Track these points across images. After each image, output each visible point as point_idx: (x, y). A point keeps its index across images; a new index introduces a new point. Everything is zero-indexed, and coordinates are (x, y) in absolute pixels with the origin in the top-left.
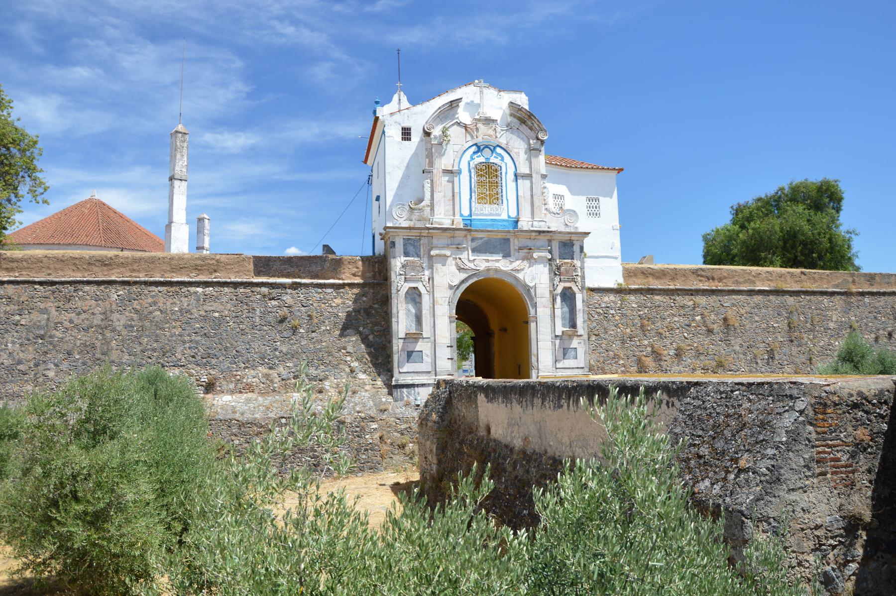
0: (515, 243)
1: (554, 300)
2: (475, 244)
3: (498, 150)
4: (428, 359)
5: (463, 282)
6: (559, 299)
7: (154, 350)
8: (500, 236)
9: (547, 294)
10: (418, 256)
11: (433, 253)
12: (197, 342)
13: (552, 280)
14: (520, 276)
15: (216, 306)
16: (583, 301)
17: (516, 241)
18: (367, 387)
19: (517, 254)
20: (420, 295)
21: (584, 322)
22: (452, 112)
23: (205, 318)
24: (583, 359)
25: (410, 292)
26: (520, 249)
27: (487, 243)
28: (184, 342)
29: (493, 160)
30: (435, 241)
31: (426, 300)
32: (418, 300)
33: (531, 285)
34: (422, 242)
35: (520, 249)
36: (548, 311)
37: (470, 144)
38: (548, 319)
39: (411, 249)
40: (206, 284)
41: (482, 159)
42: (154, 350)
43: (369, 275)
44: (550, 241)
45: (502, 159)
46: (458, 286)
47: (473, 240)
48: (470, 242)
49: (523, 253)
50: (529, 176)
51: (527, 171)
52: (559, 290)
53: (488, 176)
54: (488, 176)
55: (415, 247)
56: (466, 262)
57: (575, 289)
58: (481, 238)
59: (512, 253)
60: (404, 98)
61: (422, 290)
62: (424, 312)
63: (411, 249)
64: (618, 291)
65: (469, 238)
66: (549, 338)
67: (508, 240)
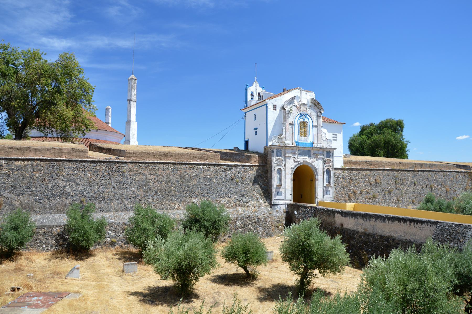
0: (312, 152)
1: (324, 173)
2: (299, 152)
3: (307, 116)
4: (283, 195)
6: (325, 173)
7: (187, 191)
9: (322, 171)
10: (281, 156)
12: (203, 188)
13: (323, 166)
14: (313, 164)
15: (208, 173)
18: (263, 205)
20: (281, 171)
23: (205, 178)
26: (314, 154)
27: (303, 151)
28: (198, 188)
29: (306, 120)
30: (287, 151)
31: (283, 172)
33: (317, 167)
35: (314, 154)
36: (322, 177)
37: (298, 113)
38: (322, 180)
39: (279, 153)
40: (204, 165)
41: (302, 120)
42: (187, 191)
43: (260, 162)
47: (299, 150)
49: (315, 155)
50: (317, 126)
51: (316, 125)
52: (325, 170)
53: (304, 125)
54: (304, 125)
57: (330, 169)
60: (258, 84)
61: (282, 169)
63: (279, 153)
64: (342, 169)
67: (310, 151)
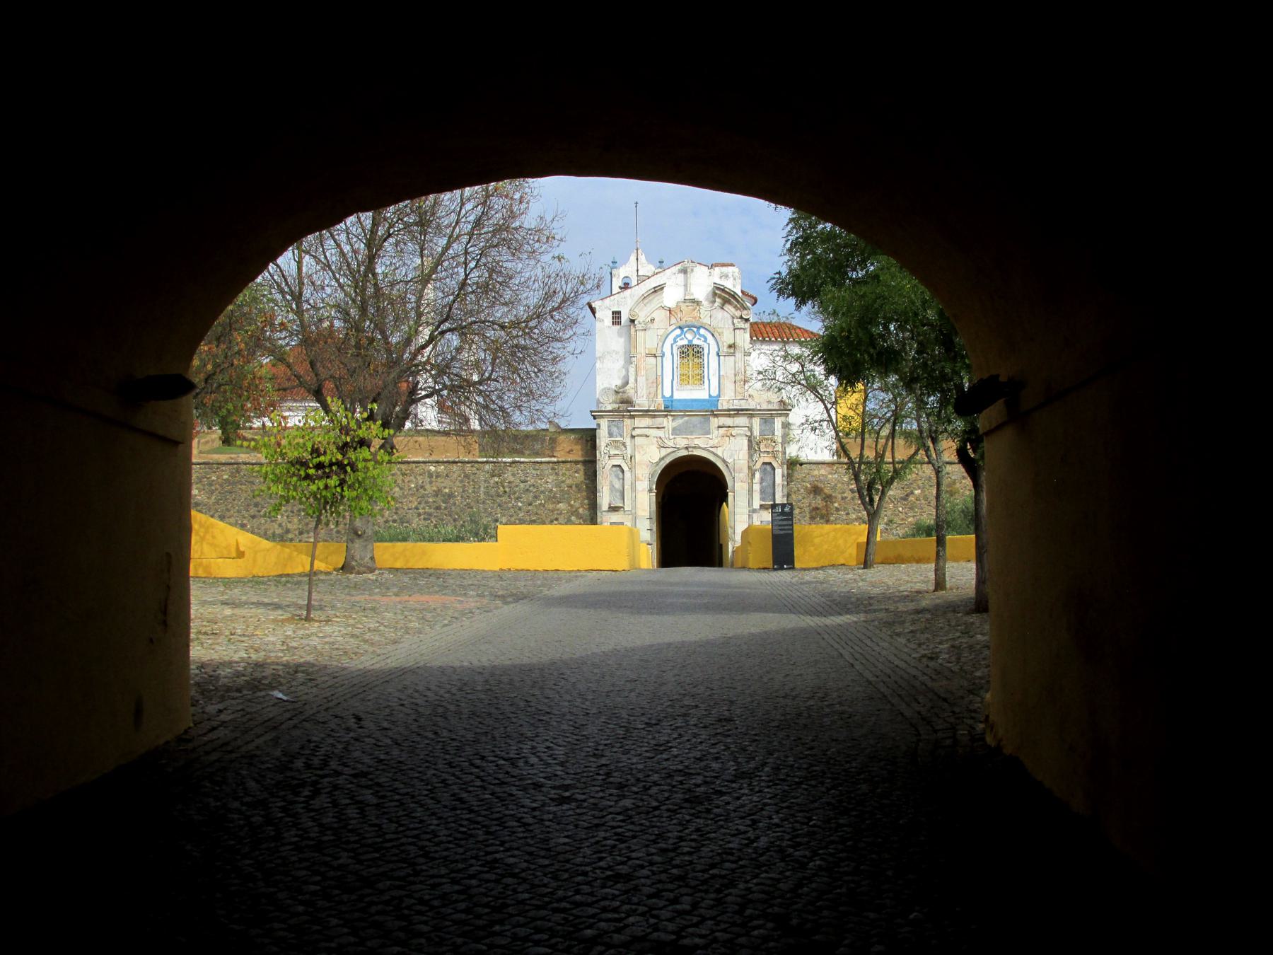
3: (702, 331)
5: (662, 459)
7: (394, 521)
9: (746, 470)
12: (430, 514)
13: (751, 456)
15: (447, 482)
20: (623, 472)
23: (437, 493)
28: (419, 515)
29: (695, 342)
31: (627, 475)
36: (746, 486)
39: (615, 430)
41: (685, 342)
42: (394, 521)
45: (705, 340)
46: (657, 463)
49: (722, 431)
52: (758, 465)
57: (775, 464)
60: (642, 258)
61: (625, 468)
63: (615, 430)
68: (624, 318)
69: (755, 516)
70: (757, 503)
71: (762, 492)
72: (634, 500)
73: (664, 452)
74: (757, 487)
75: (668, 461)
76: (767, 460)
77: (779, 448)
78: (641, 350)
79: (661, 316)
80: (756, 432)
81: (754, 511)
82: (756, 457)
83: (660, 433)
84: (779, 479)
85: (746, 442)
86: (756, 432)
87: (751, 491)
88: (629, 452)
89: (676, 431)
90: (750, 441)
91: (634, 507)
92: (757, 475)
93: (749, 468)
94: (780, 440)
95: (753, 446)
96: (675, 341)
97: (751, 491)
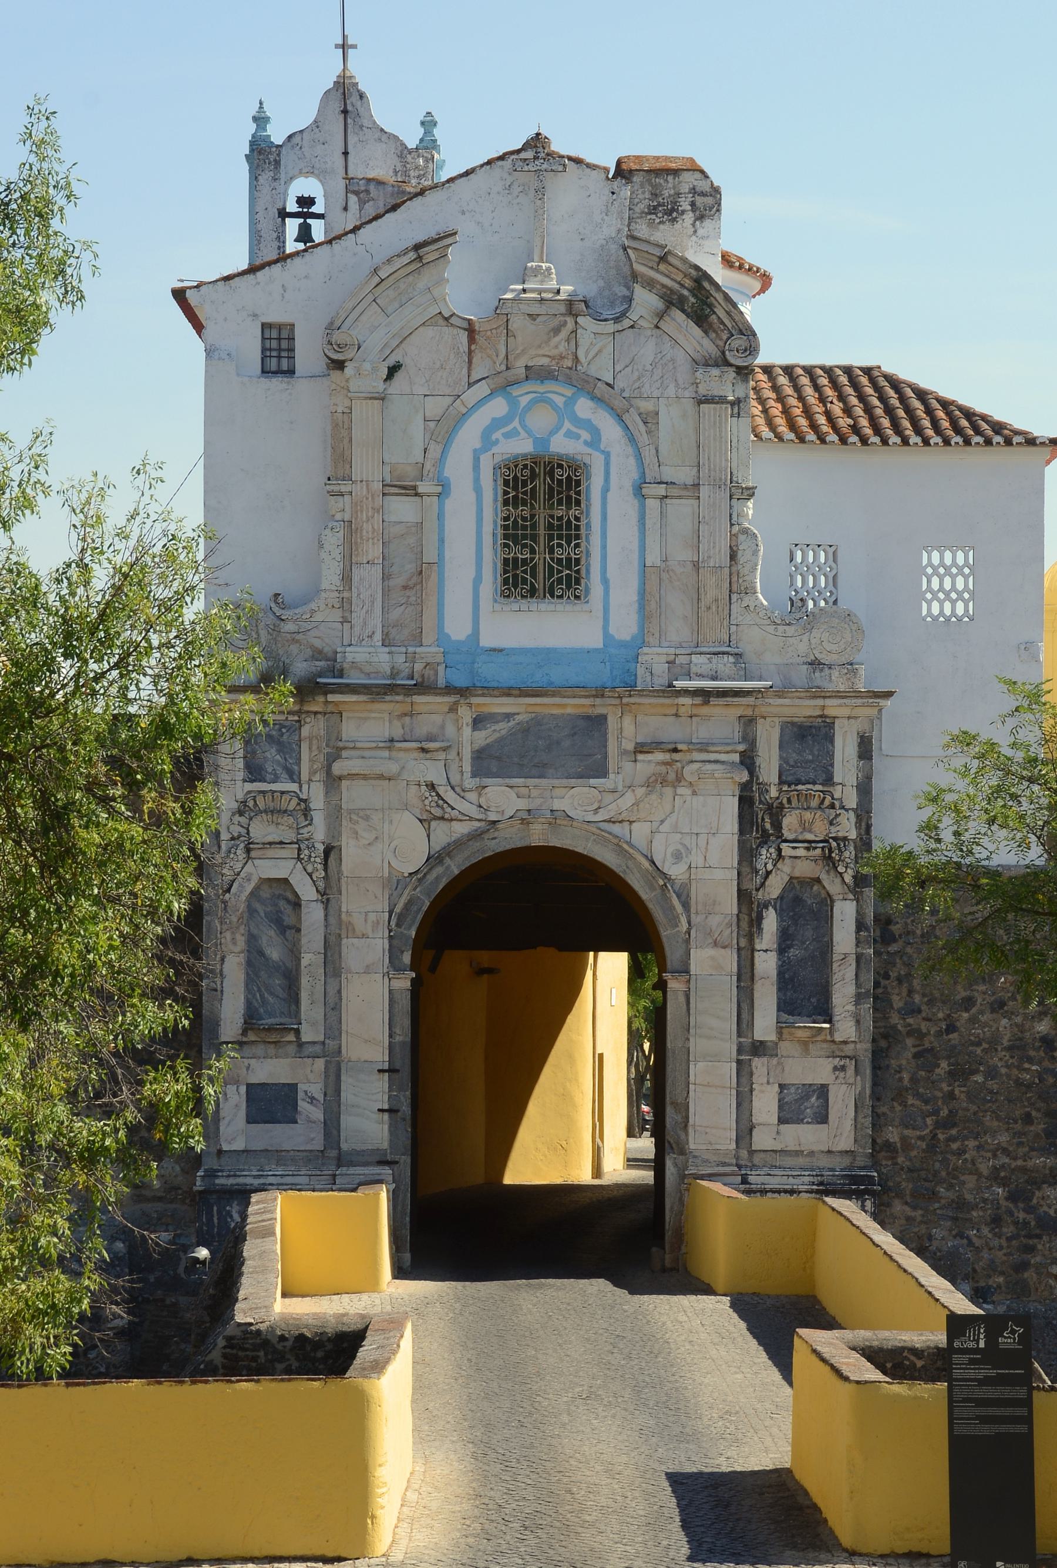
0: (624, 730)
2: (482, 737)
4: (311, 1112)
6: (771, 921)
8: (573, 706)
9: (730, 904)
10: (293, 776)
11: (337, 768)
13: (747, 855)
16: (860, 926)
17: (628, 721)
19: (628, 766)
20: (296, 904)
21: (859, 998)
22: (424, 281)
24: (848, 1124)
25: (266, 893)
26: (641, 749)
27: (525, 730)
31: (313, 916)
32: (289, 919)
34: (305, 731)
35: (641, 749)
36: (730, 960)
39: (271, 755)
41: (523, 446)
44: (749, 722)
45: (595, 442)
48: (467, 731)
49: (650, 763)
52: (775, 887)
55: (282, 747)
56: (450, 796)
57: (832, 885)
58: (508, 716)
59: (612, 765)
61: (306, 891)
62: (306, 959)
65: (466, 715)
66: (730, 1048)
67: (602, 719)
68: (308, 353)
69: (759, 1065)
70: (765, 1022)
71: (786, 980)
72: (334, 1008)
73: (443, 835)
74: (767, 964)
75: (454, 867)
76: (806, 869)
77: (847, 827)
78: (366, 468)
79: (432, 353)
80: (769, 768)
81: (759, 1049)
82: (766, 855)
83: (433, 772)
84: (844, 936)
85: (732, 805)
86: (769, 768)
87: (746, 976)
88: (319, 832)
89: (488, 763)
90: (745, 801)
91: (333, 1029)
92: (771, 921)
93: (743, 896)
94: (852, 800)
95: (758, 822)
96: (487, 436)
97: (746, 976)
